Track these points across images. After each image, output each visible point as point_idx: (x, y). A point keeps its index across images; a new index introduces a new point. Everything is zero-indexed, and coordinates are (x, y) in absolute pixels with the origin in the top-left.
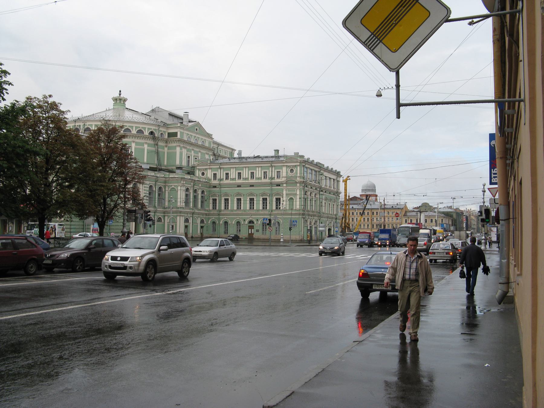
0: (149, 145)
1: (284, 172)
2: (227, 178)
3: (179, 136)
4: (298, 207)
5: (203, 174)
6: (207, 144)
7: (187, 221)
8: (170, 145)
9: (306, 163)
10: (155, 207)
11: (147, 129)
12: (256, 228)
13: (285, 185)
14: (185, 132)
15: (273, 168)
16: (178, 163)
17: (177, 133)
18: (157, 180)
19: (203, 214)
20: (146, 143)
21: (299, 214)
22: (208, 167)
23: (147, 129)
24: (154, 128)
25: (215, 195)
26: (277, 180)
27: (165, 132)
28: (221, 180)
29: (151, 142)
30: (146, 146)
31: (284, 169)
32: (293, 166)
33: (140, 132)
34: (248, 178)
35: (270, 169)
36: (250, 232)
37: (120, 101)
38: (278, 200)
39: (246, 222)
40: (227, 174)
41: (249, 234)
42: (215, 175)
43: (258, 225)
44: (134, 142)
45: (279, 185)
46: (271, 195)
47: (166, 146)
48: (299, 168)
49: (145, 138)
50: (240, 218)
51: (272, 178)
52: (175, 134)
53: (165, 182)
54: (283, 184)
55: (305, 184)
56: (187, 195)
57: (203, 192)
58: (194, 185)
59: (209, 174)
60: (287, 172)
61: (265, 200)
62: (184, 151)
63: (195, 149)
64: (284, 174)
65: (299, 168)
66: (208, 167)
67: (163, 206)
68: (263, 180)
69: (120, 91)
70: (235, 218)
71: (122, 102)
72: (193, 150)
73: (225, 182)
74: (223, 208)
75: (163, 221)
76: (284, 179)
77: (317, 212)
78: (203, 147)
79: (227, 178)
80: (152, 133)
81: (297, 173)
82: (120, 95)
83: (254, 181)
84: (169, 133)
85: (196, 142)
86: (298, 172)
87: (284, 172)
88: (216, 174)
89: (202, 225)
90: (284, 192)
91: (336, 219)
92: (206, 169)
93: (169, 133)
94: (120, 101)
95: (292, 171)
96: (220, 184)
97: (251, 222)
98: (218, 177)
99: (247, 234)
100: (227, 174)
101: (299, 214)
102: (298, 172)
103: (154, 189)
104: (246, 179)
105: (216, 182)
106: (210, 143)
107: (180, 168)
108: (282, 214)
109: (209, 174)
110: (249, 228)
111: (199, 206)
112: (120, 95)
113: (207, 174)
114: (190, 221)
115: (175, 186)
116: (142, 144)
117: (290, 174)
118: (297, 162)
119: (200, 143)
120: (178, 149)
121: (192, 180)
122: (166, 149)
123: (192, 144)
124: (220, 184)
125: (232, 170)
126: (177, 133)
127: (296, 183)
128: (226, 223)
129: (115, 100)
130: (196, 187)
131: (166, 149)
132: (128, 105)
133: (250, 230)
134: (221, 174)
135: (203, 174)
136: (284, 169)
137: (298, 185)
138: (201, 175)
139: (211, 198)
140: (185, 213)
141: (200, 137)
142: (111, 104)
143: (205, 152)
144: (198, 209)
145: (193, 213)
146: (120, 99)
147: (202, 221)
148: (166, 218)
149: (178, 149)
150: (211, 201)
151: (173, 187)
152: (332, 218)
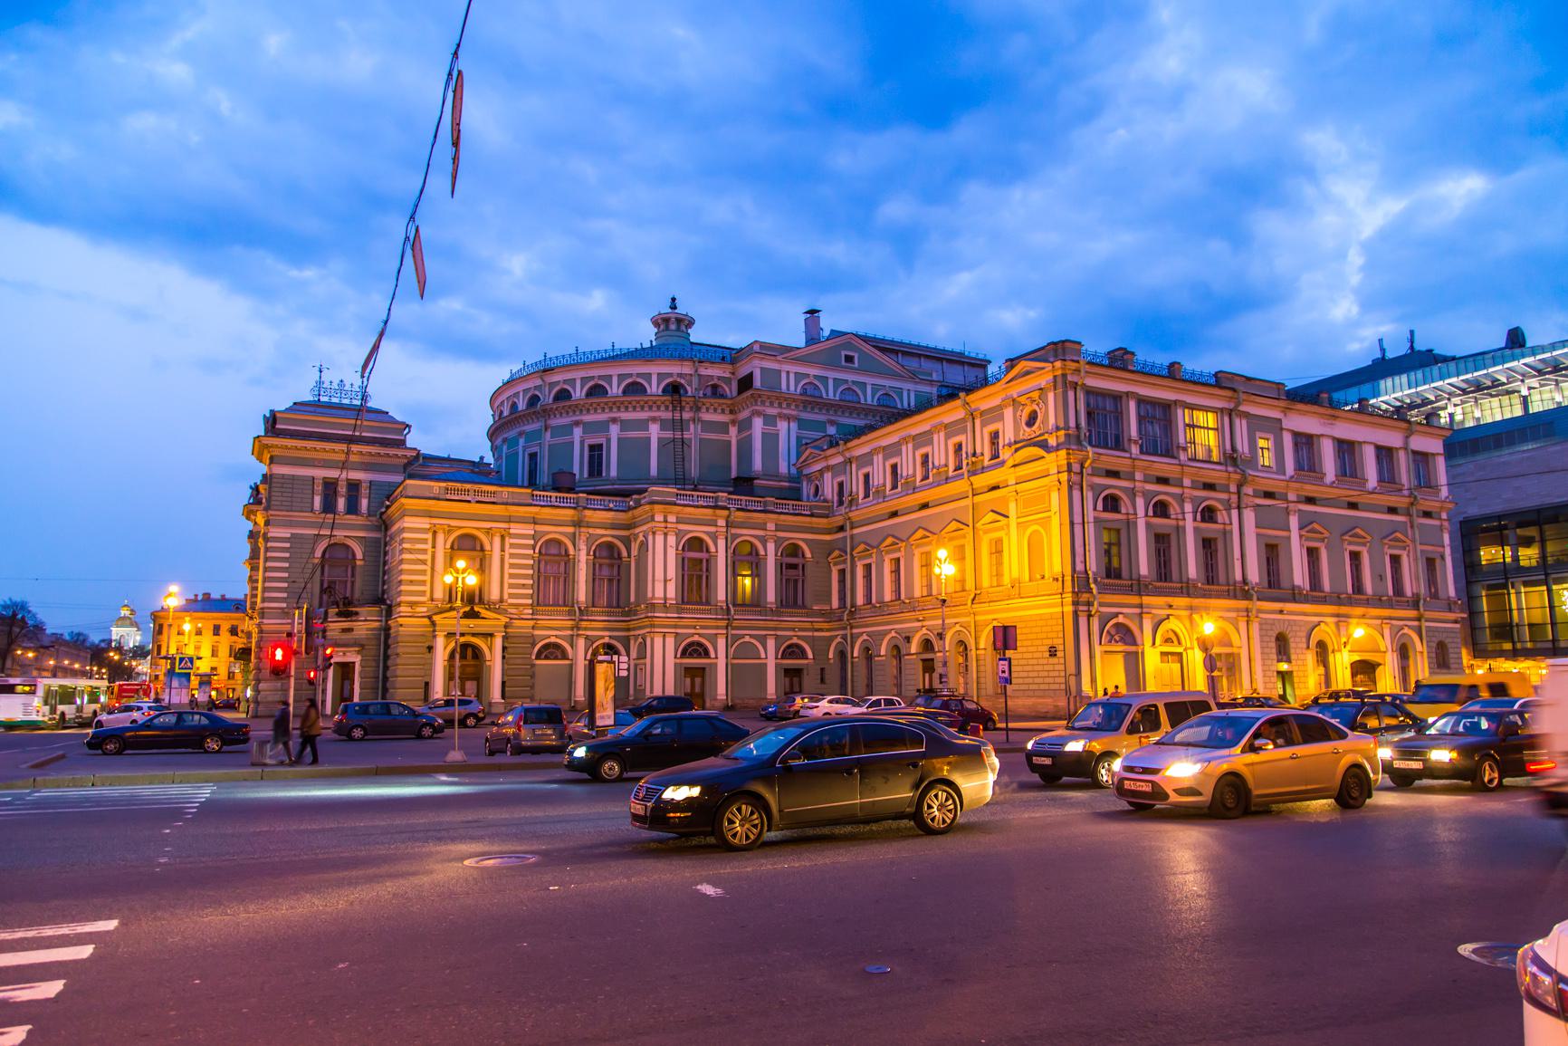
0: (664, 425)
3: (757, 382)
14: (786, 367)
15: (978, 422)
17: (751, 375)
23: (654, 379)
27: (728, 381)
29: (667, 415)
30: (654, 431)
37: (673, 324)
47: (733, 422)
69: (674, 300)
71: (673, 327)
82: (674, 307)
94: (673, 324)
116: (643, 425)
122: (733, 431)
126: (751, 375)
129: (656, 324)
132: (696, 335)
141: (869, 380)
146: (666, 321)
149: (758, 423)
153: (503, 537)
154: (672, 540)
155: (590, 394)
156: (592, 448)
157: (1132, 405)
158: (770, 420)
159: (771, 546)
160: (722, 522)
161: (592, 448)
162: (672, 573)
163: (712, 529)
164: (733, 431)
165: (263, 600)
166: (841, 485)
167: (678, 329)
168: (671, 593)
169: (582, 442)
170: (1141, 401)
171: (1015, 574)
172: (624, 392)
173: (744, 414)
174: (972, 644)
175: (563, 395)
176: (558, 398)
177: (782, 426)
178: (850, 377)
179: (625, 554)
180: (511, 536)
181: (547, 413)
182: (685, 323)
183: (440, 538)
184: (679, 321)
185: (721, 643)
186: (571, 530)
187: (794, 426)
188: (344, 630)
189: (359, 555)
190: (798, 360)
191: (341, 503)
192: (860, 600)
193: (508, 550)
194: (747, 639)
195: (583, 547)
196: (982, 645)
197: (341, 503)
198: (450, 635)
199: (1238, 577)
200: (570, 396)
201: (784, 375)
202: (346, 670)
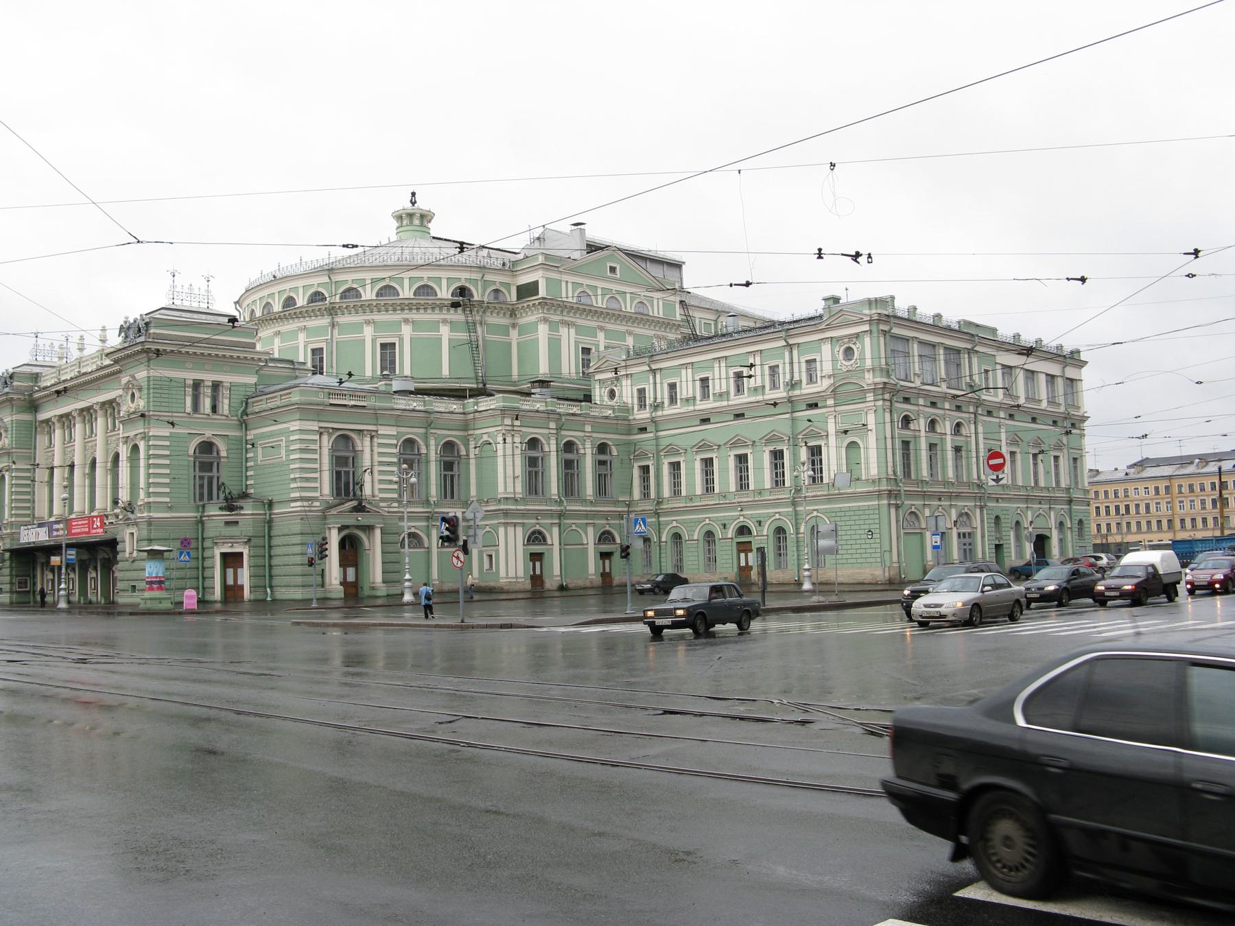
0: (453, 325)
1: (827, 358)
2: (673, 400)
3: (542, 292)
4: (874, 471)
5: (612, 394)
6: (657, 311)
7: (536, 537)
8: (522, 321)
9: (887, 320)
10: (427, 502)
11: (444, 282)
13: (830, 402)
14: (565, 277)
15: (795, 352)
16: (543, 369)
17: (536, 284)
18: (429, 421)
19: (606, 516)
20: (445, 321)
21: (879, 495)
23: (444, 282)
24: (467, 275)
25: (644, 456)
26: (807, 389)
27: (508, 285)
28: (657, 406)
30: (445, 331)
31: (826, 348)
32: (850, 337)
33: (425, 290)
34: (728, 393)
35: (787, 354)
36: (743, 564)
37: (414, 219)
38: (816, 452)
39: (730, 533)
40: (672, 386)
41: (740, 568)
43: (762, 537)
44: (406, 321)
47: (514, 326)
48: (867, 340)
50: (711, 520)
52: (532, 289)
53: (466, 427)
55: (894, 394)
56: (532, 462)
57: (602, 448)
58: (559, 429)
59: (627, 392)
60: (834, 360)
61: (777, 455)
63: (609, 326)
64: (827, 368)
65: (867, 340)
67: (463, 498)
68: (770, 395)
69: (413, 194)
71: (417, 222)
72: (601, 328)
73: (668, 411)
74: (666, 492)
76: (826, 383)
77: (969, 484)
78: (641, 318)
79: (673, 400)
80: (463, 291)
81: (863, 359)
82: (413, 203)
83: (745, 398)
85: (614, 305)
86: (868, 355)
87: (827, 358)
88: (644, 389)
89: (605, 548)
91: (1070, 502)
94: (414, 219)
95: (849, 352)
96: (653, 421)
97: (743, 530)
98: (649, 400)
99: (736, 570)
100: (672, 386)
101: (879, 495)
102: (868, 355)
103: (424, 451)
105: (642, 415)
106: (668, 306)
107: (543, 383)
108: (830, 499)
109: (627, 392)
110: (739, 551)
111: (589, 488)
112: (413, 203)
113: (621, 396)
114: (553, 537)
116: (435, 326)
117: (844, 365)
118: (862, 322)
119: (629, 307)
120: (543, 329)
121: (553, 412)
123: (563, 307)
124: (653, 421)
125: (684, 371)
126: (536, 284)
127: (864, 391)
128: (677, 537)
129: (399, 218)
130: (568, 435)
131: (514, 334)
132: (435, 228)
133: (742, 555)
134: (658, 390)
135: (612, 394)
136: (826, 348)
137: (870, 397)
138: (606, 399)
139: (636, 465)
140: (525, 514)
142: (387, 230)
143: (594, 324)
144: (584, 502)
145: (561, 515)
146: (411, 216)
147: (605, 537)
150: (636, 473)
151: (485, 438)
152: (1051, 501)
153: (372, 437)
154: (517, 440)
156: (383, 346)
157: (942, 351)
158: (553, 326)
159: (588, 445)
160: (552, 425)
161: (383, 346)
162: (518, 471)
163: (546, 431)
164: (514, 334)
165: (149, 494)
166: (642, 392)
167: (422, 225)
168: (519, 489)
169: (374, 341)
170: (947, 348)
172: (415, 294)
174: (790, 530)
175: (350, 293)
176: (344, 295)
177: (563, 331)
178: (615, 287)
179: (463, 452)
180: (379, 436)
181: (332, 311)
182: (425, 217)
183: (325, 437)
184: (422, 216)
185: (556, 530)
186: (423, 431)
187: (572, 331)
188: (227, 523)
189: (223, 454)
190: (574, 271)
191: (206, 404)
192: (666, 492)
193: (376, 450)
194: (574, 527)
195: (433, 448)
196: (802, 530)
197: (206, 404)
198: (340, 530)
199: (975, 476)
200: (359, 295)
201: (564, 284)
202: (232, 560)
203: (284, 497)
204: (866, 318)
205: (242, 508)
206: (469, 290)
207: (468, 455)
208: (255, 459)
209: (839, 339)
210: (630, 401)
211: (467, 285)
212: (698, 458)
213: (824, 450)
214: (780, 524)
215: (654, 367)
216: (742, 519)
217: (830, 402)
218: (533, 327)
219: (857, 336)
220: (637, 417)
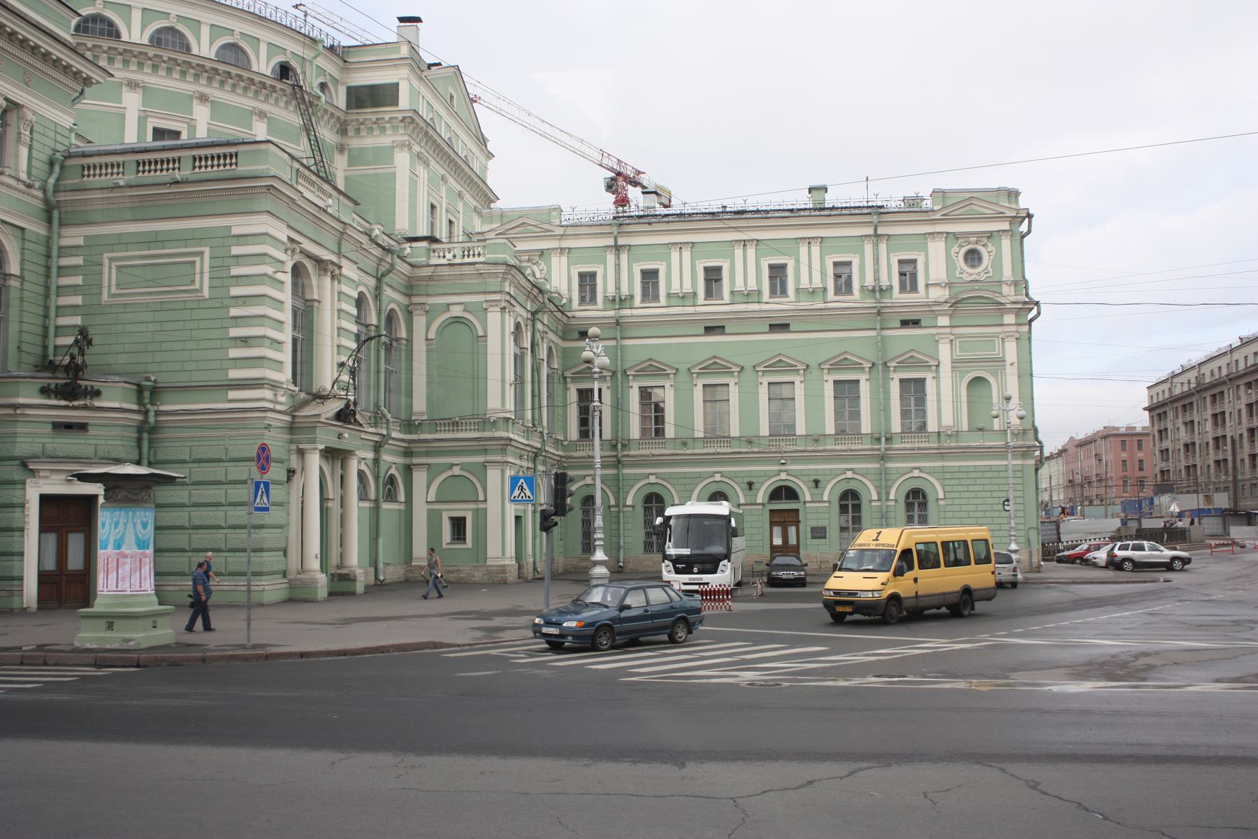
3: (404, 101)
8: (355, 143)
12: (808, 521)
13: (944, 321)
22: (554, 244)
27: (336, 82)
31: (937, 249)
34: (759, 292)
38: (914, 390)
39: (762, 496)
42: (587, 280)
43: (819, 507)
44: (203, 98)
45: (916, 323)
46: (881, 367)
47: (341, 149)
49: (256, 86)
51: (879, 291)
54: (936, 314)
62: (421, 170)
66: (554, 244)
70: (701, 477)
75: (402, 497)
80: (284, 71)
81: (997, 262)
84: (350, 90)
88: (593, 275)
90: (944, 352)
92: (542, 253)
93: (350, 90)
95: (973, 257)
97: (784, 492)
98: (606, 286)
104: (750, 296)
110: (772, 524)
115: (466, 307)
117: (967, 273)
125: (675, 255)
136: (937, 249)
148: (420, 478)
151: (457, 311)
155: (158, 39)
169: (142, 121)
171: (947, 420)
173: (368, 142)
196: (892, 496)
200: (114, 33)
203: (183, 379)
204: (1009, 213)
205: (97, 394)
206: (294, 70)
207: (410, 341)
208: (92, 288)
209: (956, 236)
210: (564, 292)
211: (294, 64)
212: (700, 383)
213: (930, 387)
214: (852, 485)
215: (621, 241)
216: (783, 476)
217: (944, 321)
218: (384, 156)
219: (990, 235)
220: (578, 314)
